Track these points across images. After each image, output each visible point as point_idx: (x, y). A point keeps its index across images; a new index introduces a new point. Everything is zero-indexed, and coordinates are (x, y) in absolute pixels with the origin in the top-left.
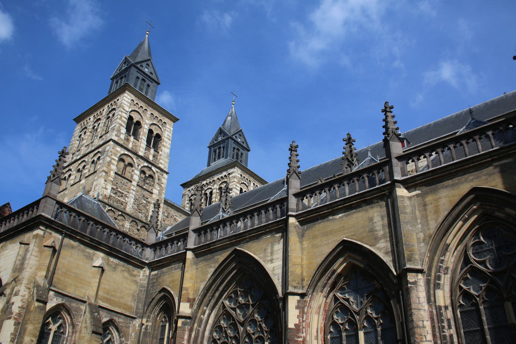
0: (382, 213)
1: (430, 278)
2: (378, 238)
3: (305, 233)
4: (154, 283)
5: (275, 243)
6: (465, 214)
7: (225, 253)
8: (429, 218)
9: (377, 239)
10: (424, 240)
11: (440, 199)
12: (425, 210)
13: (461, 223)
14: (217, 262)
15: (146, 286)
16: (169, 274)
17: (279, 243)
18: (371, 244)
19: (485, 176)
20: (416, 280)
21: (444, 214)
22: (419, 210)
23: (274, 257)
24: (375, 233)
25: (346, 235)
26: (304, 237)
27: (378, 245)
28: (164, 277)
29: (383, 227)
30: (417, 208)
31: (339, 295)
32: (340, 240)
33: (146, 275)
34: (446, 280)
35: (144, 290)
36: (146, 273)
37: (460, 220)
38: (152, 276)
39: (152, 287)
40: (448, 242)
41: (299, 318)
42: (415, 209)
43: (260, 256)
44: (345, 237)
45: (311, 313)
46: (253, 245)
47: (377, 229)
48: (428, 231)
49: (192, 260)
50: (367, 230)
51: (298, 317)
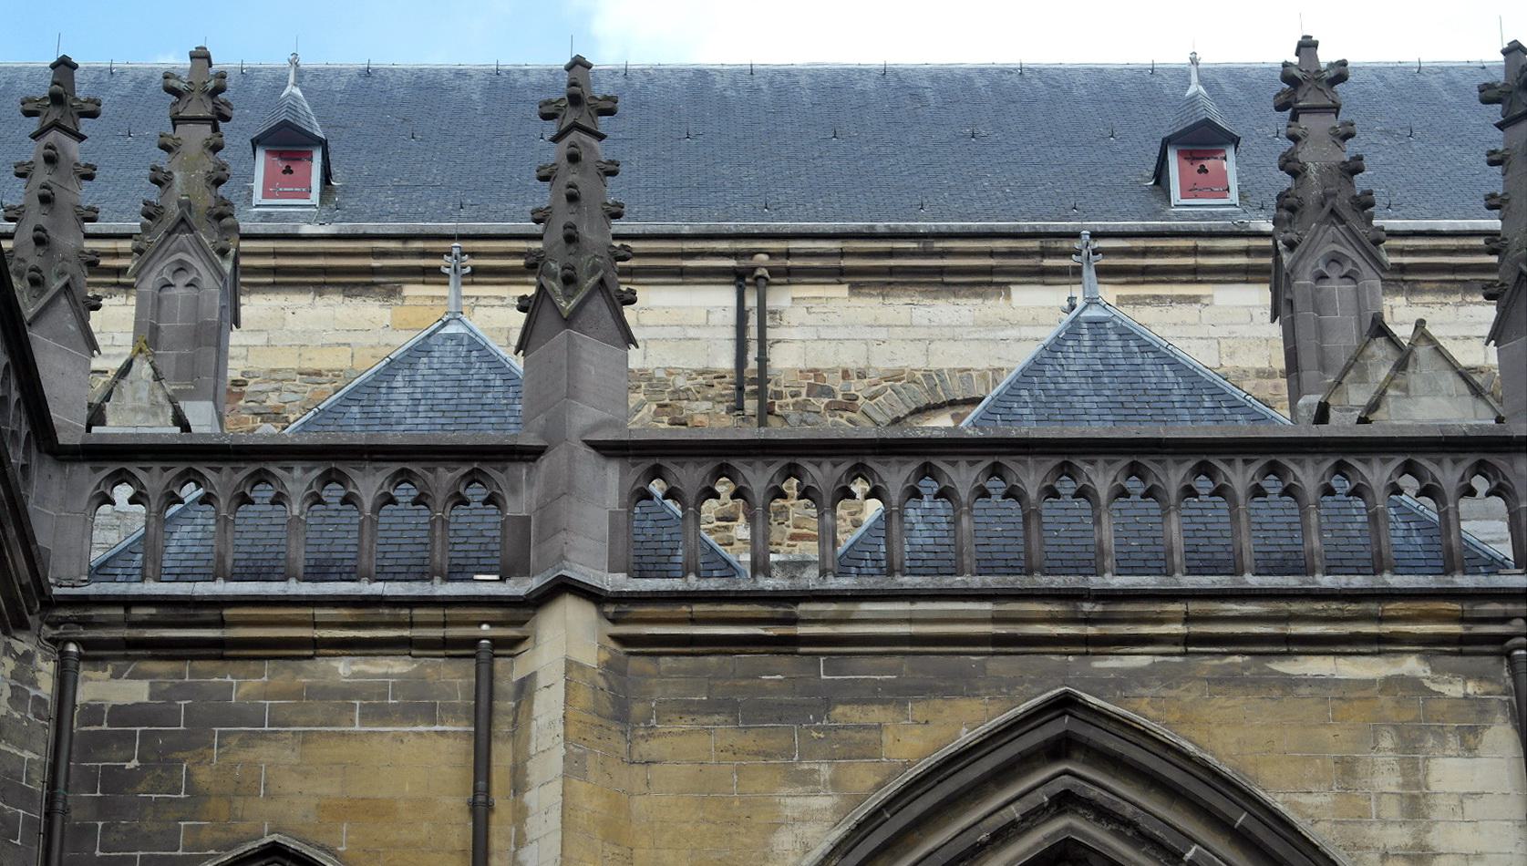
4: (116, 781)
5: (1430, 741)
7: (938, 703)
14: (868, 751)
15: (38, 787)
16: (306, 738)
23: (1435, 839)
28: (244, 755)
33: (33, 692)
35: (29, 822)
36: (33, 683)
38: (93, 713)
39: (102, 808)
43: (1304, 799)
46: (1220, 700)
49: (601, 682)
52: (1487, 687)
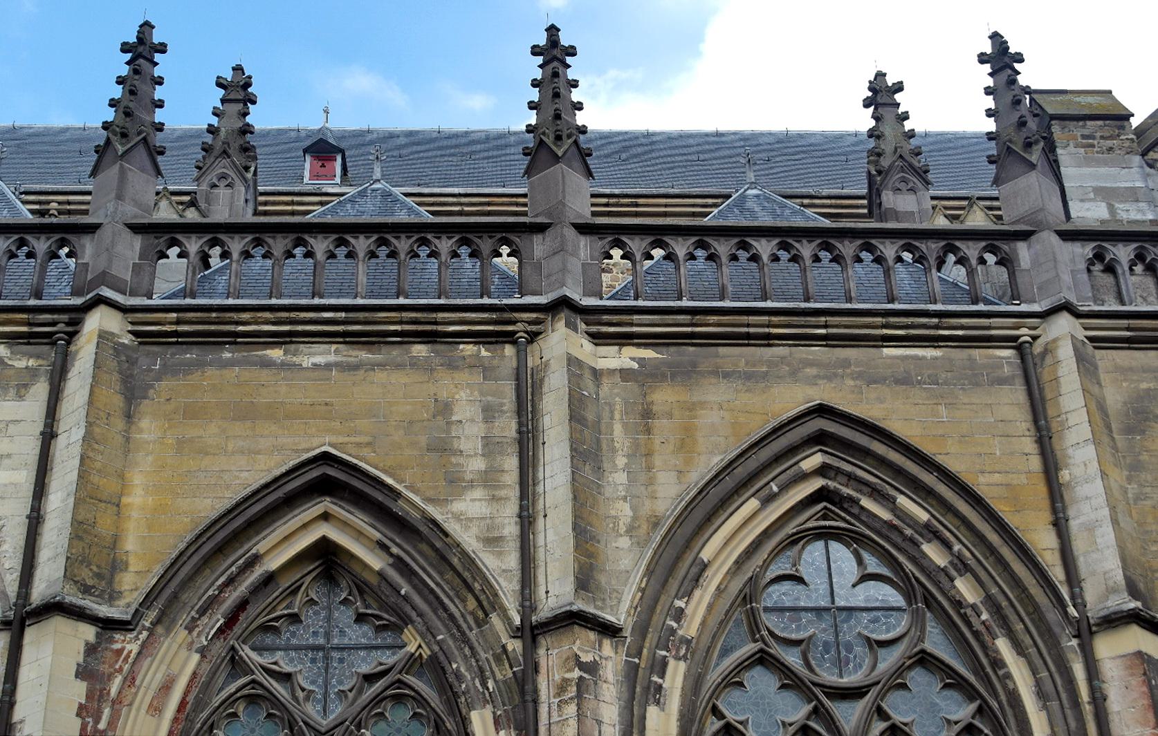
0: (490, 398)
1: (637, 660)
2: (464, 480)
3: (152, 386)
6: (772, 480)
8: (658, 461)
9: (456, 483)
10: (630, 530)
11: (702, 409)
12: (648, 431)
13: (753, 504)
17: (20, 397)
18: (430, 493)
19: (853, 379)
20: (597, 659)
21: (709, 462)
22: (625, 425)
24: (453, 460)
25: (334, 439)
26: (146, 402)
27: (458, 506)
29: (485, 446)
30: (617, 416)
31: (247, 652)
32: (308, 450)
34: (675, 677)
37: (753, 495)
40: (706, 555)
41: (83, 719)
42: (612, 418)
44: (330, 445)
45: (130, 705)
47: (462, 447)
48: (647, 503)
50: (423, 440)
51: (81, 711)
52: (40, 362)
